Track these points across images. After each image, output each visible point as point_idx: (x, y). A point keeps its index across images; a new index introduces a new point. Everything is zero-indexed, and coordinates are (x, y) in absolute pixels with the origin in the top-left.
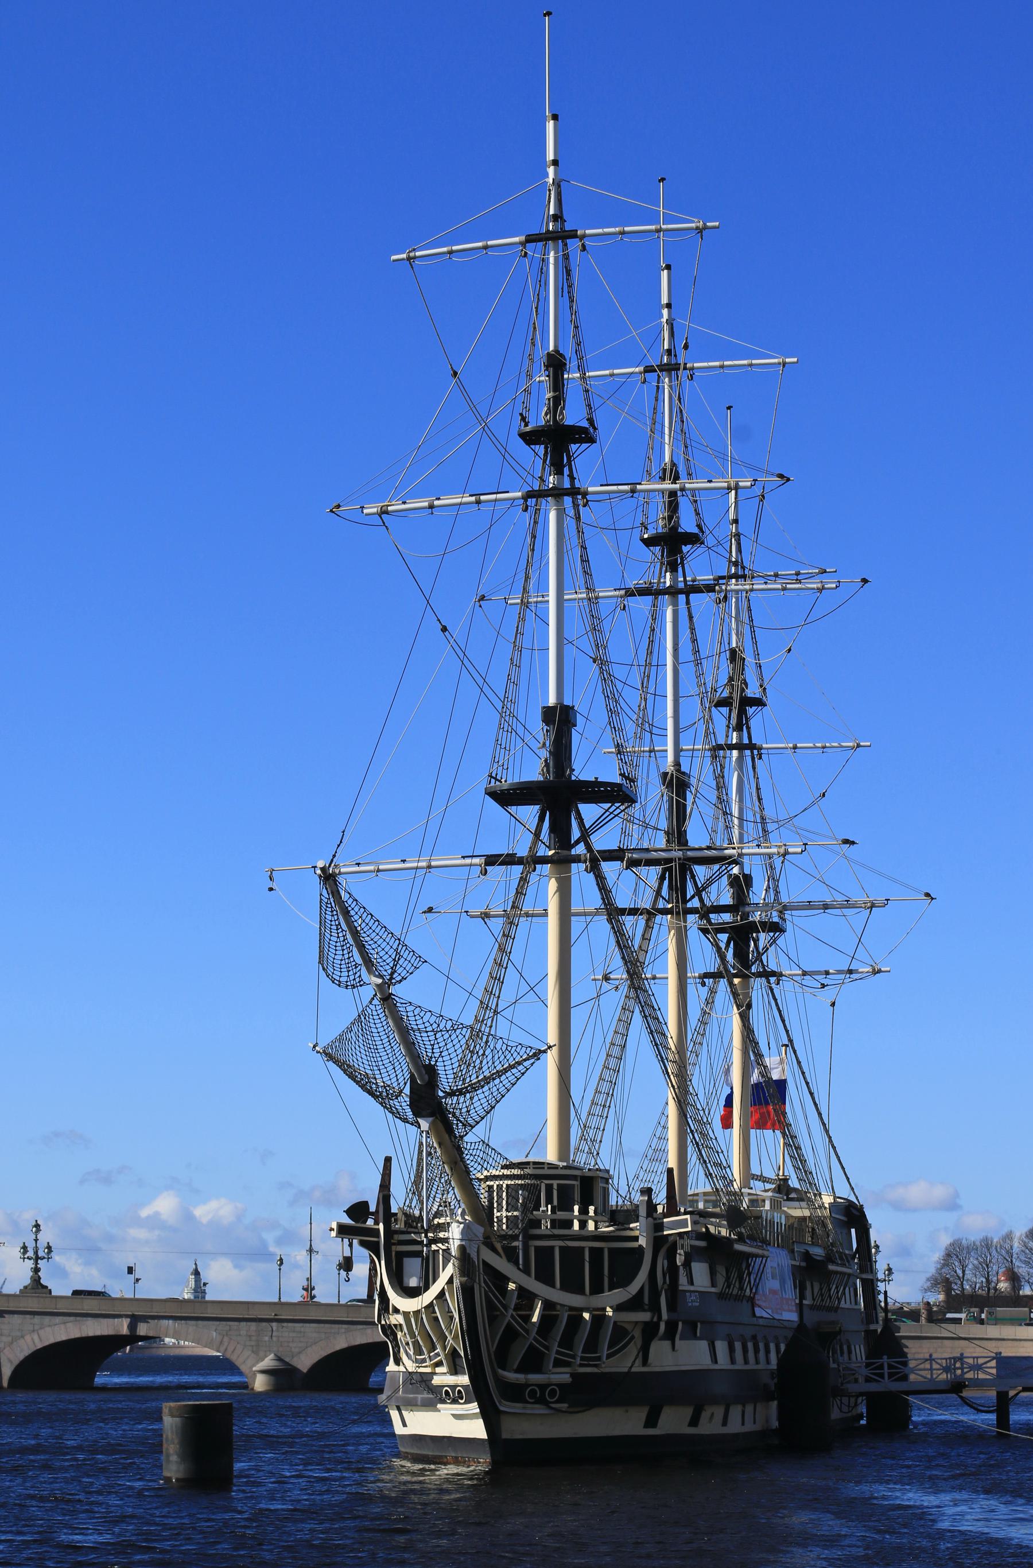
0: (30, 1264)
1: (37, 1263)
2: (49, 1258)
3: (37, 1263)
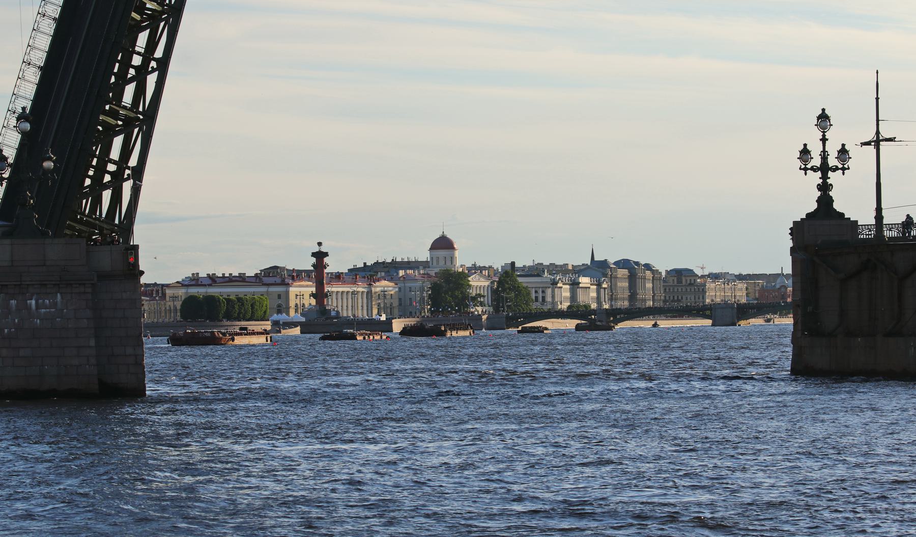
1: (825, 177)
2: (843, 169)
3: (825, 177)
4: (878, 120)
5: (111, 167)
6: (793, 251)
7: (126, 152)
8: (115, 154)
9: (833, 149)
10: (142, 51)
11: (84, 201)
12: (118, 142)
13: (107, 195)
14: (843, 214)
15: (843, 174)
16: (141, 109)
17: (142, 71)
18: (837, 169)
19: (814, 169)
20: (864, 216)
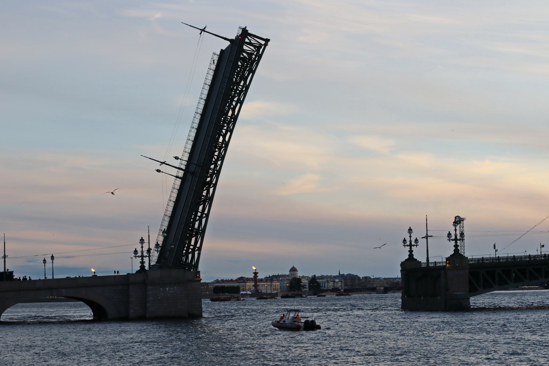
0: (453, 243)
1: (411, 248)
2: (416, 245)
3: (411, 248)
4: (427, 230)
5: (191, 247)
6: (401, 271)
7: (196, 242)
8: (193, 243)
9: (413, 240)
10: (201, 211)
12: (193, 239)
13: (190, 256)
14: (417, 259)
15: (417, 247)
16: (200, 229)
17: (201, 217)
18: (414, 245)
19: (407, 246)
20: (423, 260)
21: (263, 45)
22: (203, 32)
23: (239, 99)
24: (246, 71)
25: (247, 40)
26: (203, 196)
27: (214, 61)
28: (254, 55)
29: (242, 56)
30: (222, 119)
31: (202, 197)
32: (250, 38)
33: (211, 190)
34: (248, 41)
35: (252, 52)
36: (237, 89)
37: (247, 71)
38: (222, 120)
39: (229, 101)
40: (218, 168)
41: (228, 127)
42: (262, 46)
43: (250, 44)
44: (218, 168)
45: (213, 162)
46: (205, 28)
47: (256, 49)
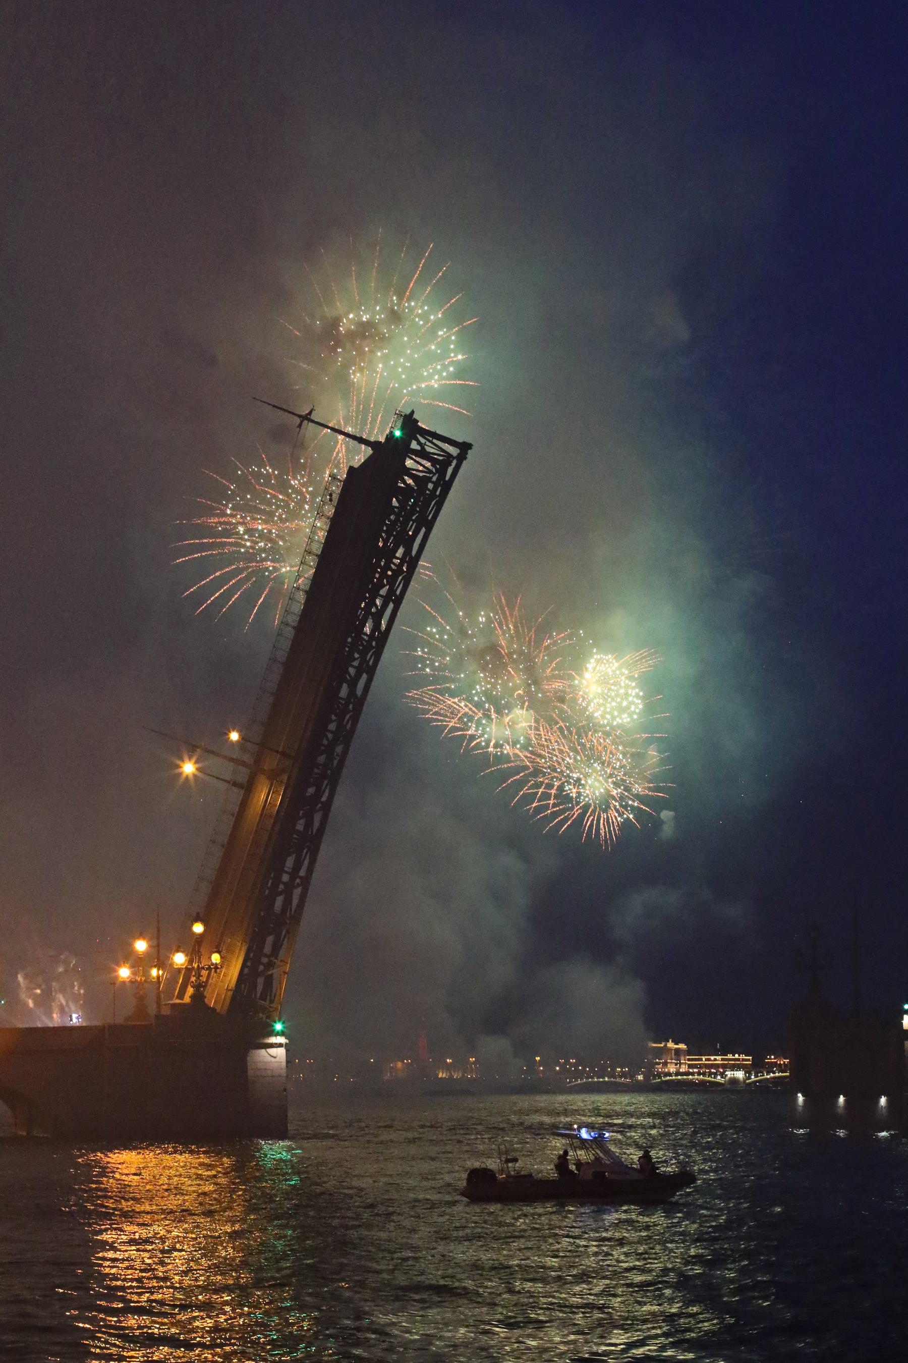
5: (265, 960)
8: (267, 949)
11: (243, 986)
12: (270, 940)
13: (261, 981)
17: (289, 888)
21: (454, 458)
22: (306, 422)
23: (391, 592)
24: (411, 523)
25: (414, 445)
26: (298, 832)
27: (331, 495)
28: (432, 482)
29: (402, 485)
30: (349, 640)
31: (295, 836)
32: (422, 440)
33: (317, 818)
34: (418, 448)
35: (428, 475)
36: (387, 567)
37: (414, 521)
38: (349, 643)
39: (367, 595)
40: (335, 762)
41: (363, 660)
42: (452, 462)
43: (423, 454)
44: (335, 762)
45: (323, 748)
46: (310, 413)
47: (438, 466)
